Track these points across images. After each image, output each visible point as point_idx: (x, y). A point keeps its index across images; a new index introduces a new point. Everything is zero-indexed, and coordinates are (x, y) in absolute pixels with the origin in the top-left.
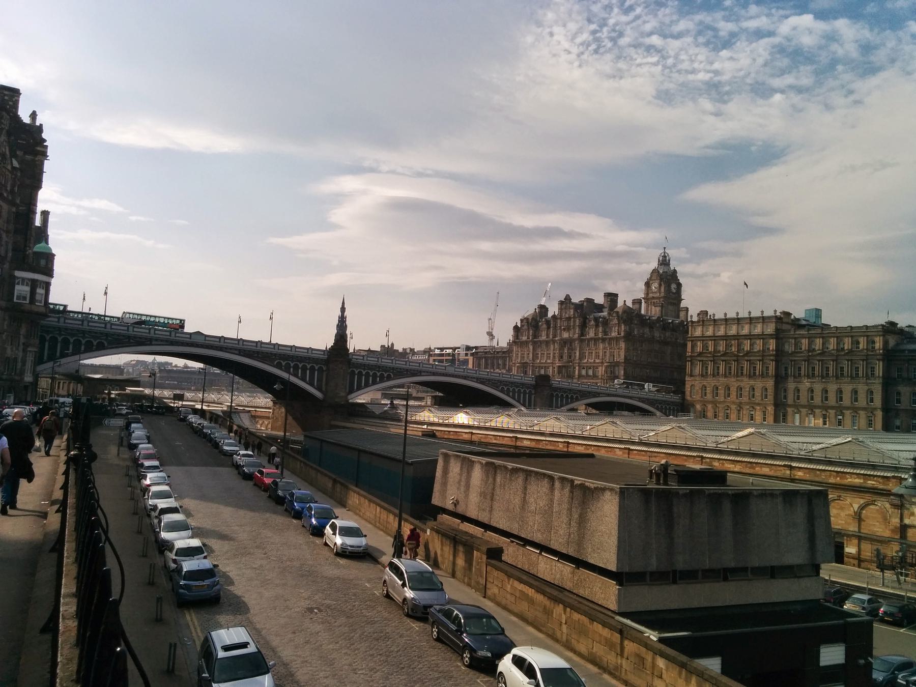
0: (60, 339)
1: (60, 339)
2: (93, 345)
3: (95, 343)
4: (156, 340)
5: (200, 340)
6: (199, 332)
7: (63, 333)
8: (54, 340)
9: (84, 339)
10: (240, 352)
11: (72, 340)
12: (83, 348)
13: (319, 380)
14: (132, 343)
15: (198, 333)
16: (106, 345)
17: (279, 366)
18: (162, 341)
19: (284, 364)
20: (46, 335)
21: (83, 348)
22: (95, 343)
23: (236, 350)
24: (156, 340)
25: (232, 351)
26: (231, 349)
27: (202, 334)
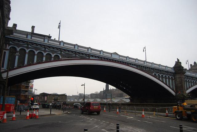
0: (27, 51)
1: (27, 51)
2: (51, 57)
3: (53, 56)
4: (92, 56)
5: (116, 57)
6: (116, 53)
7: (30, 46)
8: (23, 52)
9: (45, 52)
10: (137, 67)
11: (36, 53)
12: (44, 59)
13: (172, 85)
14: (78, 57)
15: (116, 53)
16: (60, 58)
17: (155, 76)
18: (95, 57)
19: (157, 75)
20: (17, 47)
21: (44, 59)
22: (53, 56)
23: (135, 65)
24: (92, 56)
25: (133, 66)
26: (133, 64)
27: (117, 54)
